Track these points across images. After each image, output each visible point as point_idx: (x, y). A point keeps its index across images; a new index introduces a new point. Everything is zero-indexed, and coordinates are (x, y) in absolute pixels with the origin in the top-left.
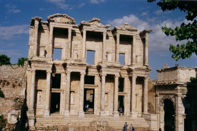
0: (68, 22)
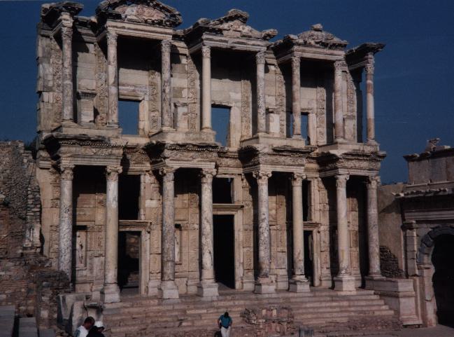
0: (162, 21)
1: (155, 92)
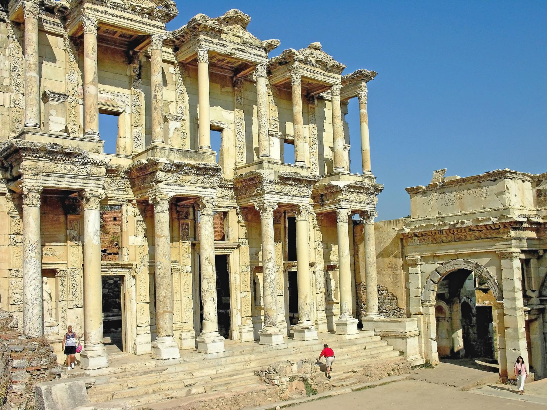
1: (139, 103)
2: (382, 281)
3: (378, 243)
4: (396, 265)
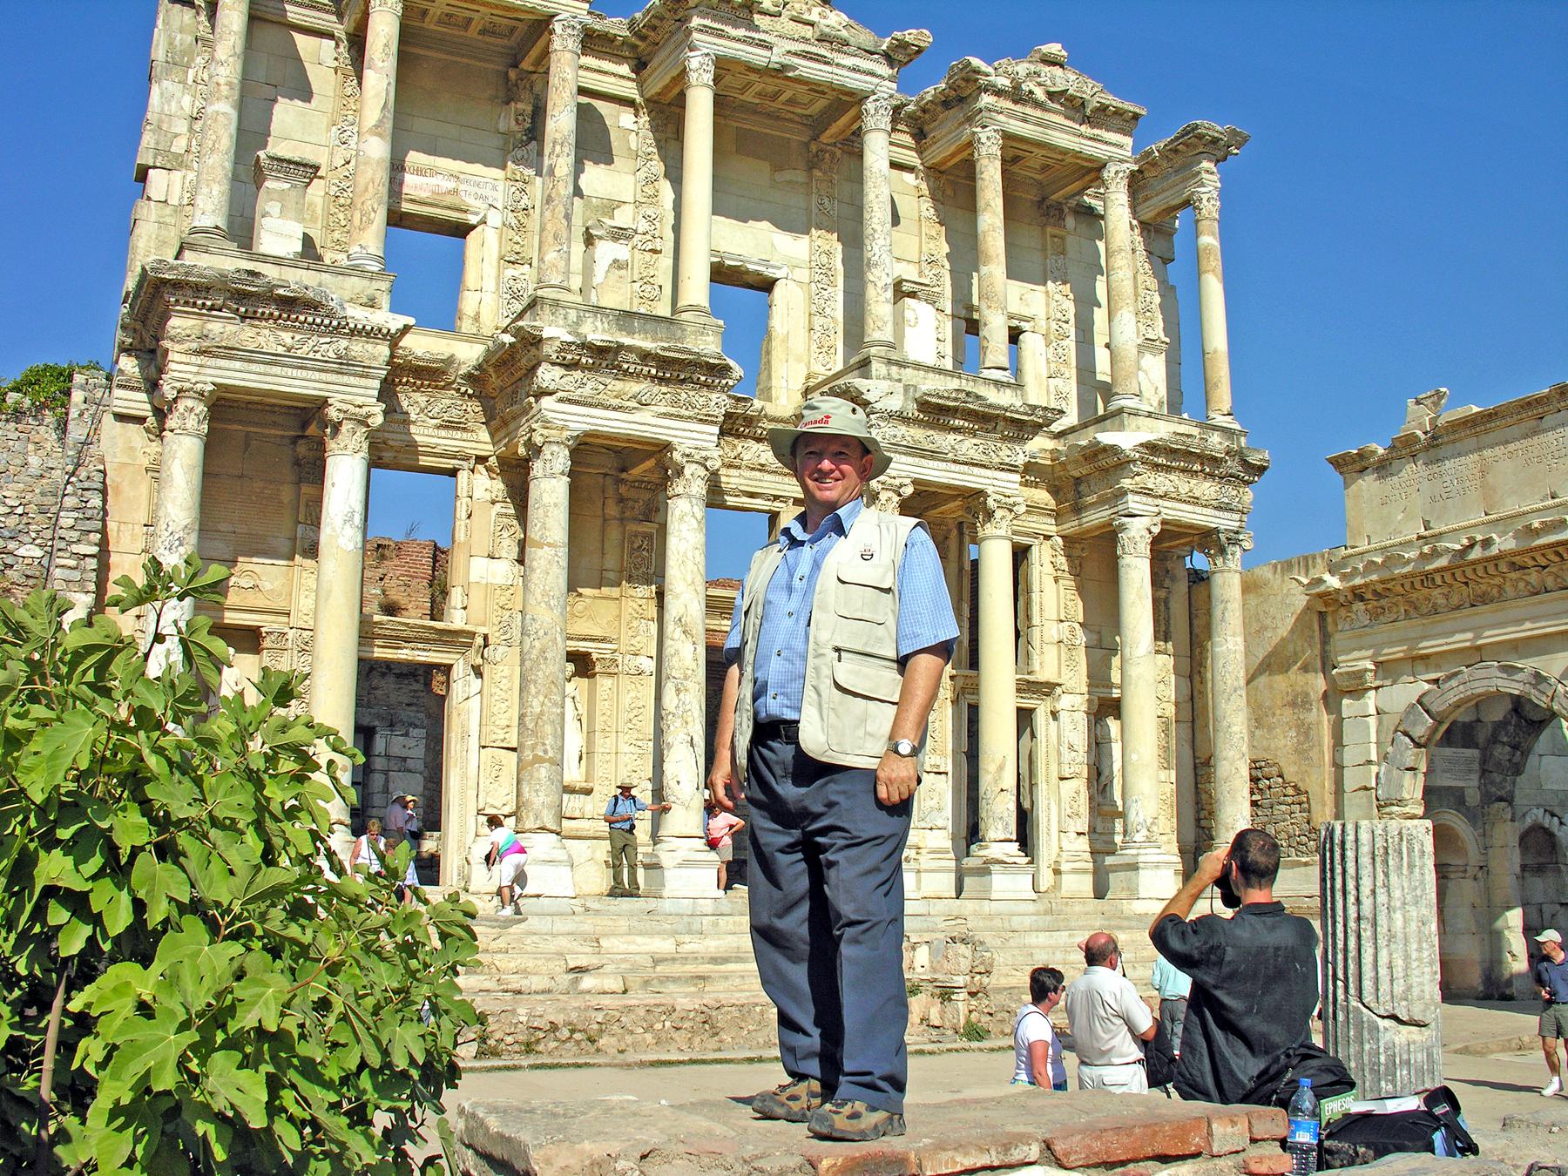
2: (1266, 750)
3: (1253, 629)
4: (1307, 695)
